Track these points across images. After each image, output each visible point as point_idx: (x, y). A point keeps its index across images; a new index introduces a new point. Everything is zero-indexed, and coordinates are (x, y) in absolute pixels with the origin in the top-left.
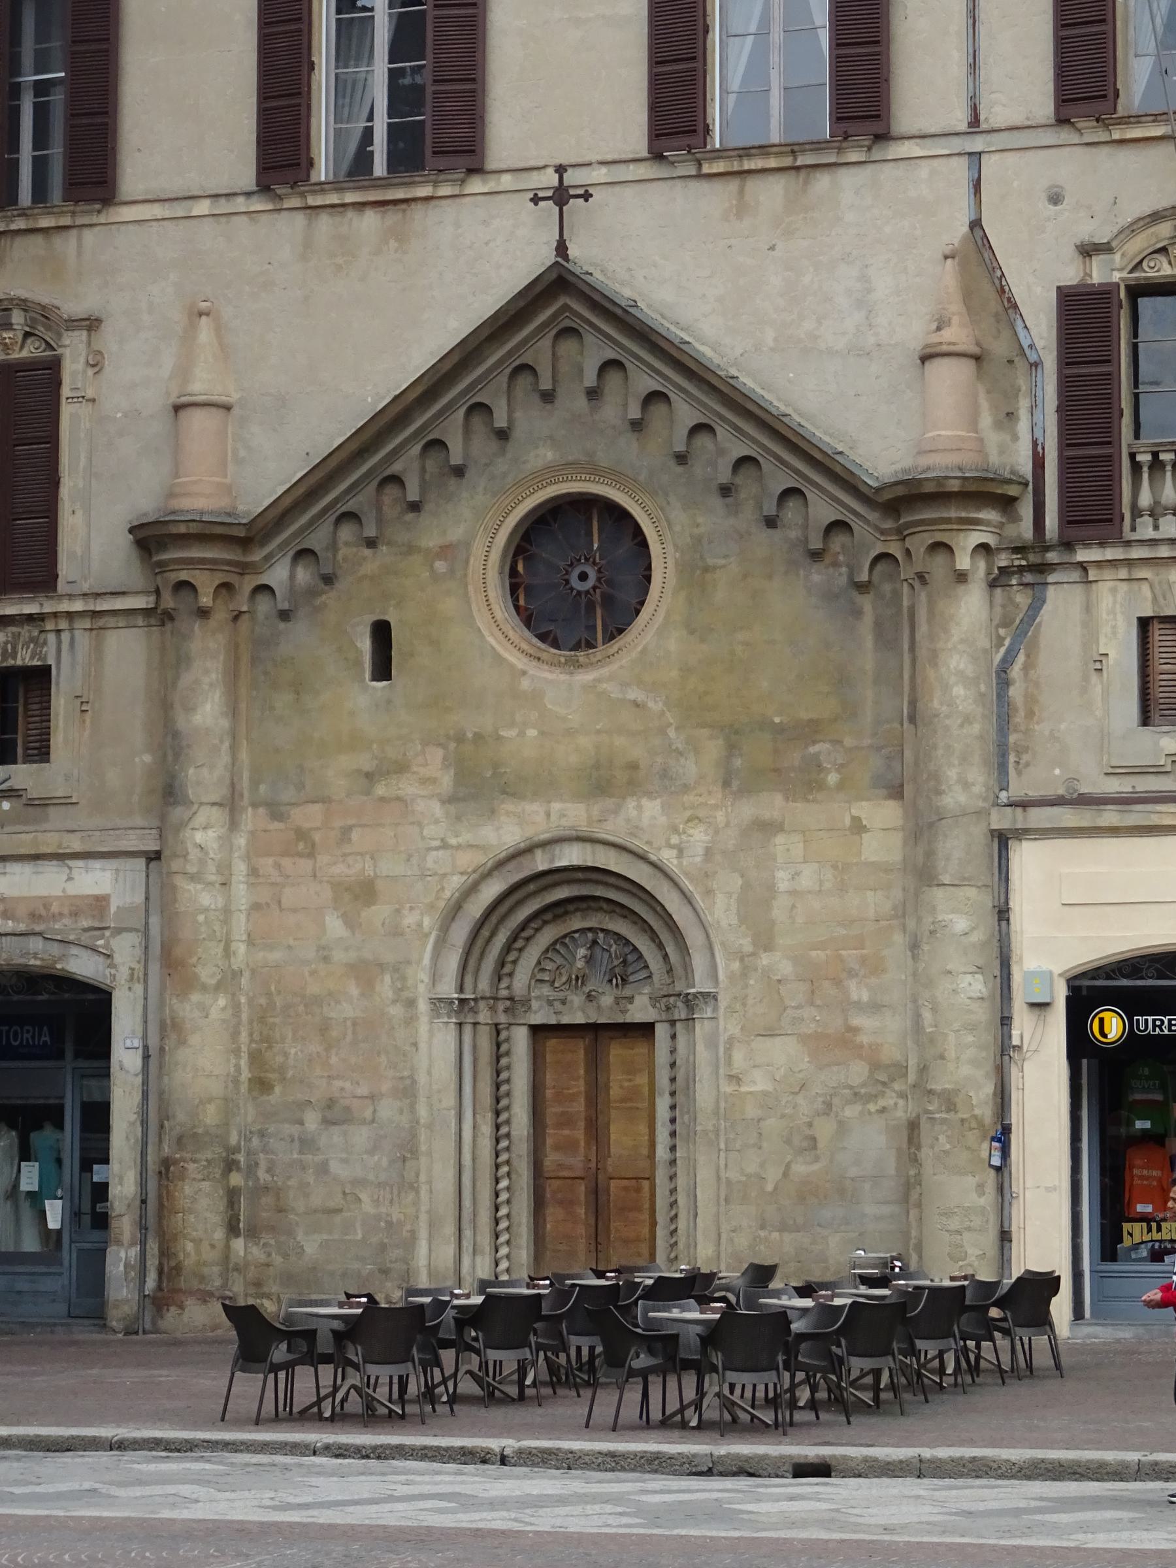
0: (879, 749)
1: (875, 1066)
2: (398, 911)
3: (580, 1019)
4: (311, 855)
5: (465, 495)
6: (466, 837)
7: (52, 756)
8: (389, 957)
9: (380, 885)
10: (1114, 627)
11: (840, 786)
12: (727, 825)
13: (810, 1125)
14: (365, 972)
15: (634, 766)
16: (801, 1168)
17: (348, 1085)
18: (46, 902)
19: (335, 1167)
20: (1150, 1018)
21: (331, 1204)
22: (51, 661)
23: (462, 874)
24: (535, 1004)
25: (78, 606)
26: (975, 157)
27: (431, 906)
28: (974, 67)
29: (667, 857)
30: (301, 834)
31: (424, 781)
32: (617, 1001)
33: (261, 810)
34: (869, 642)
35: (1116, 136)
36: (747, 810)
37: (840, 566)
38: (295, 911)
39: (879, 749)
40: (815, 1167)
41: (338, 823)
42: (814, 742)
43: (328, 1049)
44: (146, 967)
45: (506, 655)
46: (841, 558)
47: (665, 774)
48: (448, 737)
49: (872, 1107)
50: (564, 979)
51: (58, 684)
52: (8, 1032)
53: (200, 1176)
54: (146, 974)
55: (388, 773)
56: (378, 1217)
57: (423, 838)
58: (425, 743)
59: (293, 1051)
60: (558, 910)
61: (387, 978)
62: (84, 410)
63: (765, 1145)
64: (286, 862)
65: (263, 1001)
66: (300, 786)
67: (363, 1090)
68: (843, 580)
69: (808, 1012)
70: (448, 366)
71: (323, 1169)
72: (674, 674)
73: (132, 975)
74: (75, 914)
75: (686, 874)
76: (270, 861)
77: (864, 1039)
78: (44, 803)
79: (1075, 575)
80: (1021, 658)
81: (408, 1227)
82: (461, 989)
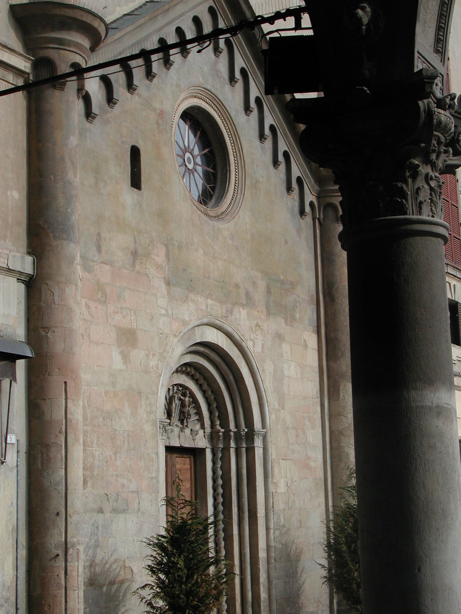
29: (248, 345)
38: (97, 344)
43: (115, 453)
59: (97, 454)
67: (133, 487)
72: (249, 236)
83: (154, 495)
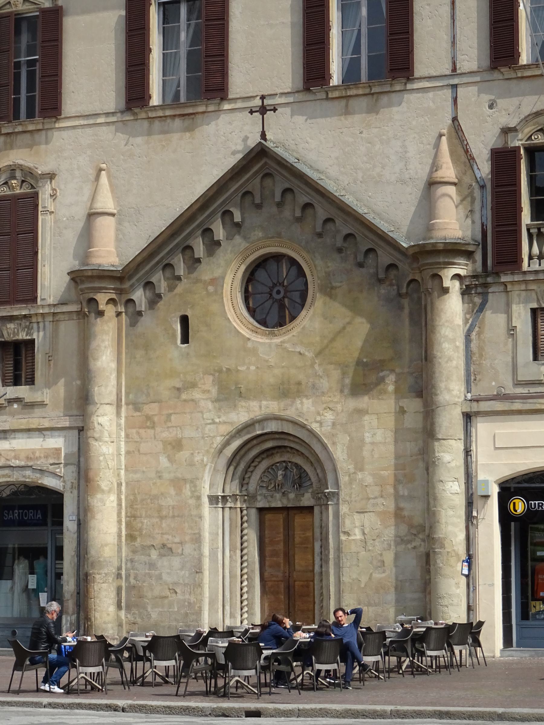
0: (412, 374)
1: (411, 526)
2: (192, 454)
3: (280, 505)
4: (153, 428)
5: (222, 254)
6: (223, 418)
7: (36, 382)
8: (188, 476)
9: (184, 442)
10: (519, 313)
12: (342, 411)
13: (381, 555)
14: (178, 483)
15: (299, 383)
16: (377, 576)
17: (170, 537)
18: (33, 451)
19: (165, 577)
20: (537, 502)
21: (163, 594)
23: (222, 436)
24: (259, 498)
25: (46, 310)
26: (454, 87)
27: (208, 451)
28: (454, 43)
29: (315, 427)
30: (148, 418)
31: (204, 392)
32: (296, 496)
33: (131, 407)
34: (407, 321)
35: (519, 75)
36: (352, 403)
37: (394, 285)
38: (145, 454)
39: (412, 374)
40: (383, 575)
41: (165, 412)
42: (382, 371)
44: (79, 482)
45: (241, 331)
46: (394, 281)
47: (314, 386)
48: (215, 371)
49: (409, 546)
50: (273, 485)
52: (22, 513)
53: (101, 581)
54: (79, 485)
55: (188, 388)
56: (184, 601)
57: (204, 419)
58: (205, 373)
59: (145, 521)
60: (268, 452)
61: (188, 486)
62: (49, 217)
63: (360, 565)
64: (142, 431)
65: (132, 497)
66: (148, 395)
67: (177, 540)
68: (394, 293)
69: (380, 501)
70: (211, 193)
71: (159, 577)
72: (318, 339)
73: (72, 486)
74: (46, 457)
75: (324, 435)
76: (134, 431)
77: (406, 513)
78: (32, 405)
79: (502, 288)
80: (477, 329)
81: (198, 605)
82: (223, 492)
83: (197, 545)
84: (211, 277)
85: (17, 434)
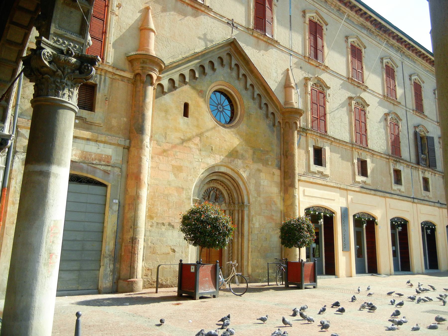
4: (167, 156)
11: (271, 165)
22: (98, 83)
43: (169, 209)
50: (207, 198)
51: (99, 90)
61: (184, 192)
65: (152, 194)
72: (244, 134)
77: (274, 218)
78: (92, 124)
84: (201, 89)
85: (77, 140)
